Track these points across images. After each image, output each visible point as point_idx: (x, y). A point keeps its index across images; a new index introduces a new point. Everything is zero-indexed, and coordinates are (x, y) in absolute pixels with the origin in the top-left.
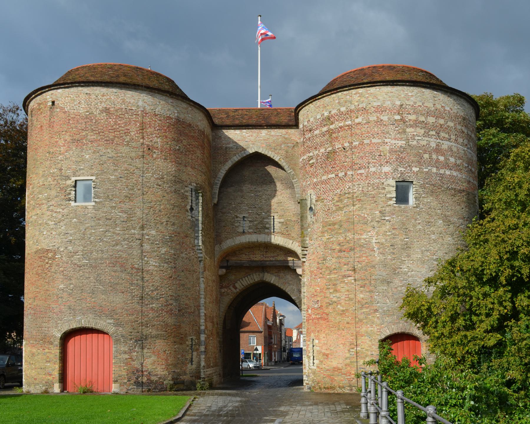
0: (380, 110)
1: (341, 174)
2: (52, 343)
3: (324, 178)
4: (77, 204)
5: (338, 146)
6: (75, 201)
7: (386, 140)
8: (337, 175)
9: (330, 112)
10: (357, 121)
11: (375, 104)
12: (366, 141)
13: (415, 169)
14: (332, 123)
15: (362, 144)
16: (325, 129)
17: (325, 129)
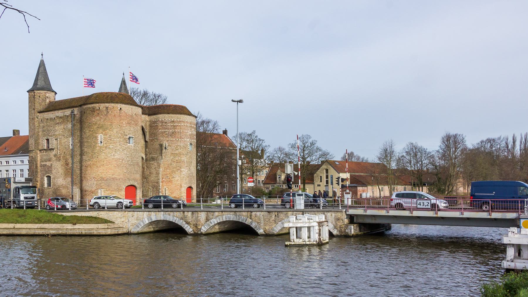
0: (187, 122)
1: (177, 139)
2: (122, 190)
3: (172, 139)
4: (129, 145)
5: (176, 131)
6: (129, 143)
7: (188, 132)
8: (176, 139)
9: (174, 120)
10: (182, 124)
11: (186, 121)
12: (184, 131)
13: (193, 140)
14: (175, 123)
15: (183, 132)
16: (172, 124)
17: (172, 124)
